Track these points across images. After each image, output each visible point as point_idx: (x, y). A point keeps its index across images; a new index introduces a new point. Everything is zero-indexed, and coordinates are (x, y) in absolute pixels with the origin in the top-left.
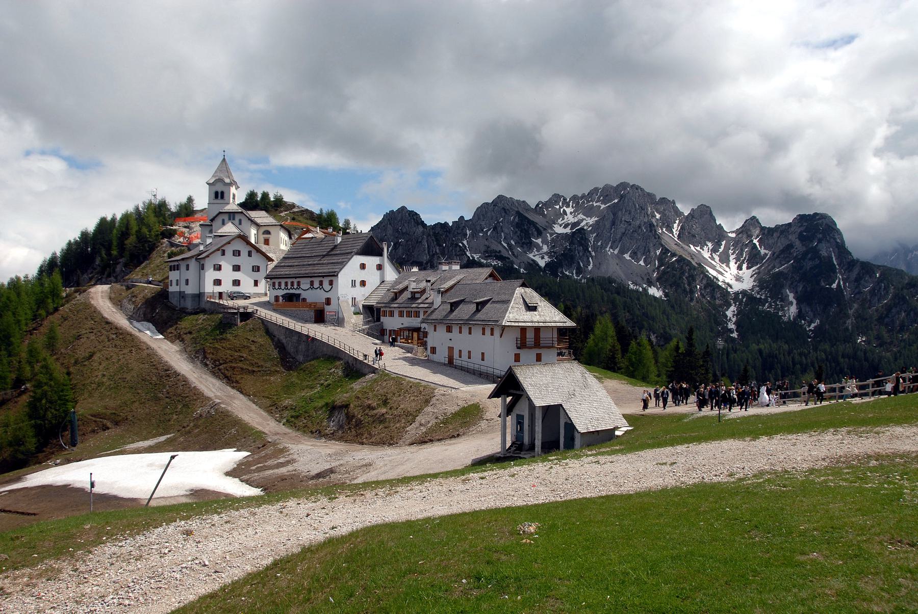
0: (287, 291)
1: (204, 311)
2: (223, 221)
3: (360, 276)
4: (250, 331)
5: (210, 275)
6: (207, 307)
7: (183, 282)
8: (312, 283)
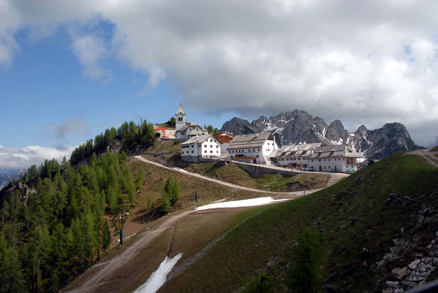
0: (237, 154)
1: (202, 162)
2: (191, 129)
3: (268, 147)
4: (232, 167)
5: (203, 149)
6: (203, 161)
7: (190, 152)
8: (249, 150)
